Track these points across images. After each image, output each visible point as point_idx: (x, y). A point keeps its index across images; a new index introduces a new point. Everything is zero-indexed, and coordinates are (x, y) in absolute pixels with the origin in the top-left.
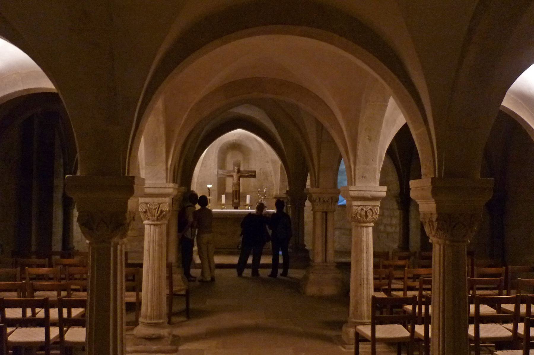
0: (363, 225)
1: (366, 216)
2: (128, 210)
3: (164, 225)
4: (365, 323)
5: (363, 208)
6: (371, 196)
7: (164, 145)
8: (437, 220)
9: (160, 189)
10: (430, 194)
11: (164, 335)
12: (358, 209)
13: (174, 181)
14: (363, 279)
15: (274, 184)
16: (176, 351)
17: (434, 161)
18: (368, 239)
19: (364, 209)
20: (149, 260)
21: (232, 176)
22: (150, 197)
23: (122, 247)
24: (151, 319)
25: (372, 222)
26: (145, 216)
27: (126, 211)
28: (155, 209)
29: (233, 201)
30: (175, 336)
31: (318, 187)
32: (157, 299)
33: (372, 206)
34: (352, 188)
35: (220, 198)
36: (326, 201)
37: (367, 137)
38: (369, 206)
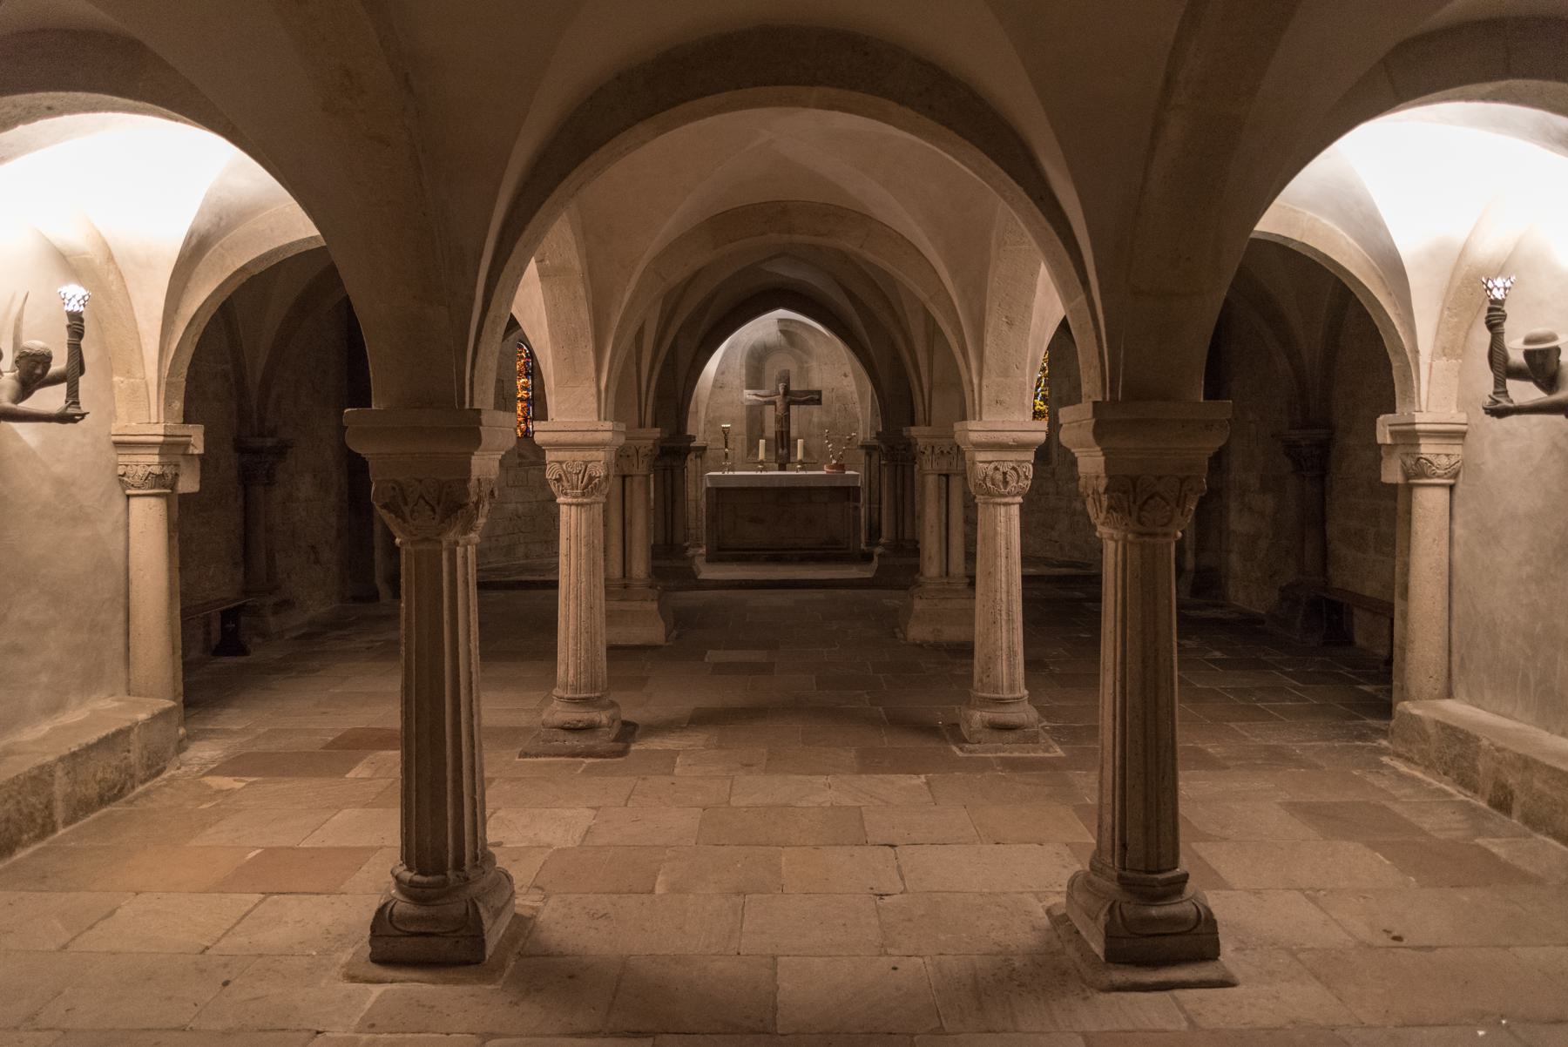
1: (1006, 483)
2: (474, 478)
3: (596, 505)
6: (1014, 442)
7: (591, 345)
8: (1107, 490)
10: (1091, 437)
11: (600, 722)
13: (617, 417)
16: (623, 753)
17: (1103, 365)
18: (1008, 529)
21: (774, 403)
22: (566, 450)
23: (466, 550)
24: (575, 690)
25: (1018, 494)
26: (558, 486)
27: (467, 480)
28: (577, 474)
30: (625, 724)
31: (930, 425)
32: (587, 651)
33: (1017, 461)
34: (972, 425)
35: (752, 447)
36: (945, 452)
37: (1004, 319)
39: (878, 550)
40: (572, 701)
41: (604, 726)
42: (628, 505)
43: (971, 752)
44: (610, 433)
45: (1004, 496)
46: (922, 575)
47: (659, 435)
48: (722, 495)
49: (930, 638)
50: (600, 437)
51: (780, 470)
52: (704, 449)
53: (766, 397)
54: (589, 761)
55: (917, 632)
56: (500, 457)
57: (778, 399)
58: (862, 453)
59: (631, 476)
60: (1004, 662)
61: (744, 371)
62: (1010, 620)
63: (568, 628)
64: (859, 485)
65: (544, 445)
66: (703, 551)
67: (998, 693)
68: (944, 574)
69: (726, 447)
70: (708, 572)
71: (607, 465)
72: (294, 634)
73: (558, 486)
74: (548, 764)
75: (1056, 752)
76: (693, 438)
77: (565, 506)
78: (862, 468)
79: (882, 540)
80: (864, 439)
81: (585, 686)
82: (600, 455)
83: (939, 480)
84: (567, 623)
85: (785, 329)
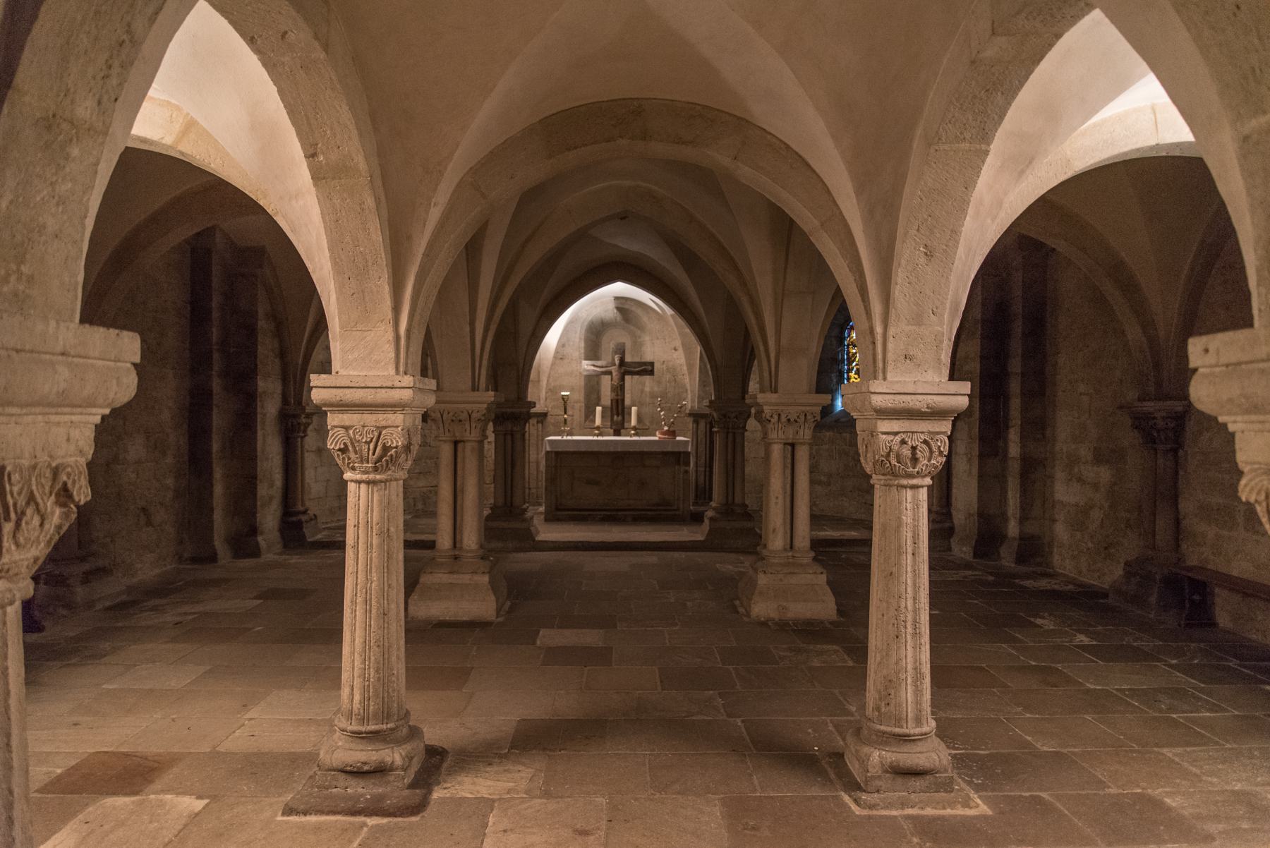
0: (905, 482)
1: (915, 460)
4: (909, 736)
5: (906, 439)
6: (928, 408)
9: (379, 390)
11: (393, 762)
12: (892, 441)
14: (905, 622)
15: (689, 388)
16: (417, 808)
18: (916, 519)
19: (909, 443)
20: (357, 572)
21: (610, 373)
24: (362, 721)
26: (344, 459)
28: (368, 443)
29: (612, 419)
31: (776, 392)
32: (377, 671)
33: (930, 433)
34: (877, 386)
35: (590, 414)
38: (922, 432)
39: (710, 513)
40: (357, 735)
41: (397, 769)
42: (459, 472)
43: (871, 807)
44: (411, 391)
45: (911, 476)
46: (765, 546)
47: (493, 399)
48: (560, 457)
49: (774, 614)
50: (396, 395)
51: (615, 435)
52: (545, 415)
53: (602, 367)
54: (372, 821)
55: (761, 609)
56: (98, 419)
57: (614, 369)
58: (690, 420)
59: (463, 441)
60: (909, 687)
61: (582, 345)
62: (916, 634)
63: (354, 640)
64: (689, 450)
65: (325, 405)
66: (542, 509)
67: (902, 727)
68: (788, 547)
69: (565, 413)
70: (548, 533)
71: (409, 433)
72: (108, 604)
73: (344, 459)
74: (317, 828)
75: (977, 806)
76: (533, 404)
77: (353, 483)
78: (690, 433)
79: (713, 504)
80: (692, 407)
81: (375, 715)
82: (397, 419)
83: (784, 447)
84: (353, 633)
85: (620, 306)
